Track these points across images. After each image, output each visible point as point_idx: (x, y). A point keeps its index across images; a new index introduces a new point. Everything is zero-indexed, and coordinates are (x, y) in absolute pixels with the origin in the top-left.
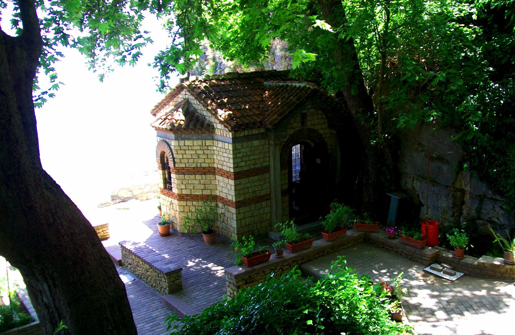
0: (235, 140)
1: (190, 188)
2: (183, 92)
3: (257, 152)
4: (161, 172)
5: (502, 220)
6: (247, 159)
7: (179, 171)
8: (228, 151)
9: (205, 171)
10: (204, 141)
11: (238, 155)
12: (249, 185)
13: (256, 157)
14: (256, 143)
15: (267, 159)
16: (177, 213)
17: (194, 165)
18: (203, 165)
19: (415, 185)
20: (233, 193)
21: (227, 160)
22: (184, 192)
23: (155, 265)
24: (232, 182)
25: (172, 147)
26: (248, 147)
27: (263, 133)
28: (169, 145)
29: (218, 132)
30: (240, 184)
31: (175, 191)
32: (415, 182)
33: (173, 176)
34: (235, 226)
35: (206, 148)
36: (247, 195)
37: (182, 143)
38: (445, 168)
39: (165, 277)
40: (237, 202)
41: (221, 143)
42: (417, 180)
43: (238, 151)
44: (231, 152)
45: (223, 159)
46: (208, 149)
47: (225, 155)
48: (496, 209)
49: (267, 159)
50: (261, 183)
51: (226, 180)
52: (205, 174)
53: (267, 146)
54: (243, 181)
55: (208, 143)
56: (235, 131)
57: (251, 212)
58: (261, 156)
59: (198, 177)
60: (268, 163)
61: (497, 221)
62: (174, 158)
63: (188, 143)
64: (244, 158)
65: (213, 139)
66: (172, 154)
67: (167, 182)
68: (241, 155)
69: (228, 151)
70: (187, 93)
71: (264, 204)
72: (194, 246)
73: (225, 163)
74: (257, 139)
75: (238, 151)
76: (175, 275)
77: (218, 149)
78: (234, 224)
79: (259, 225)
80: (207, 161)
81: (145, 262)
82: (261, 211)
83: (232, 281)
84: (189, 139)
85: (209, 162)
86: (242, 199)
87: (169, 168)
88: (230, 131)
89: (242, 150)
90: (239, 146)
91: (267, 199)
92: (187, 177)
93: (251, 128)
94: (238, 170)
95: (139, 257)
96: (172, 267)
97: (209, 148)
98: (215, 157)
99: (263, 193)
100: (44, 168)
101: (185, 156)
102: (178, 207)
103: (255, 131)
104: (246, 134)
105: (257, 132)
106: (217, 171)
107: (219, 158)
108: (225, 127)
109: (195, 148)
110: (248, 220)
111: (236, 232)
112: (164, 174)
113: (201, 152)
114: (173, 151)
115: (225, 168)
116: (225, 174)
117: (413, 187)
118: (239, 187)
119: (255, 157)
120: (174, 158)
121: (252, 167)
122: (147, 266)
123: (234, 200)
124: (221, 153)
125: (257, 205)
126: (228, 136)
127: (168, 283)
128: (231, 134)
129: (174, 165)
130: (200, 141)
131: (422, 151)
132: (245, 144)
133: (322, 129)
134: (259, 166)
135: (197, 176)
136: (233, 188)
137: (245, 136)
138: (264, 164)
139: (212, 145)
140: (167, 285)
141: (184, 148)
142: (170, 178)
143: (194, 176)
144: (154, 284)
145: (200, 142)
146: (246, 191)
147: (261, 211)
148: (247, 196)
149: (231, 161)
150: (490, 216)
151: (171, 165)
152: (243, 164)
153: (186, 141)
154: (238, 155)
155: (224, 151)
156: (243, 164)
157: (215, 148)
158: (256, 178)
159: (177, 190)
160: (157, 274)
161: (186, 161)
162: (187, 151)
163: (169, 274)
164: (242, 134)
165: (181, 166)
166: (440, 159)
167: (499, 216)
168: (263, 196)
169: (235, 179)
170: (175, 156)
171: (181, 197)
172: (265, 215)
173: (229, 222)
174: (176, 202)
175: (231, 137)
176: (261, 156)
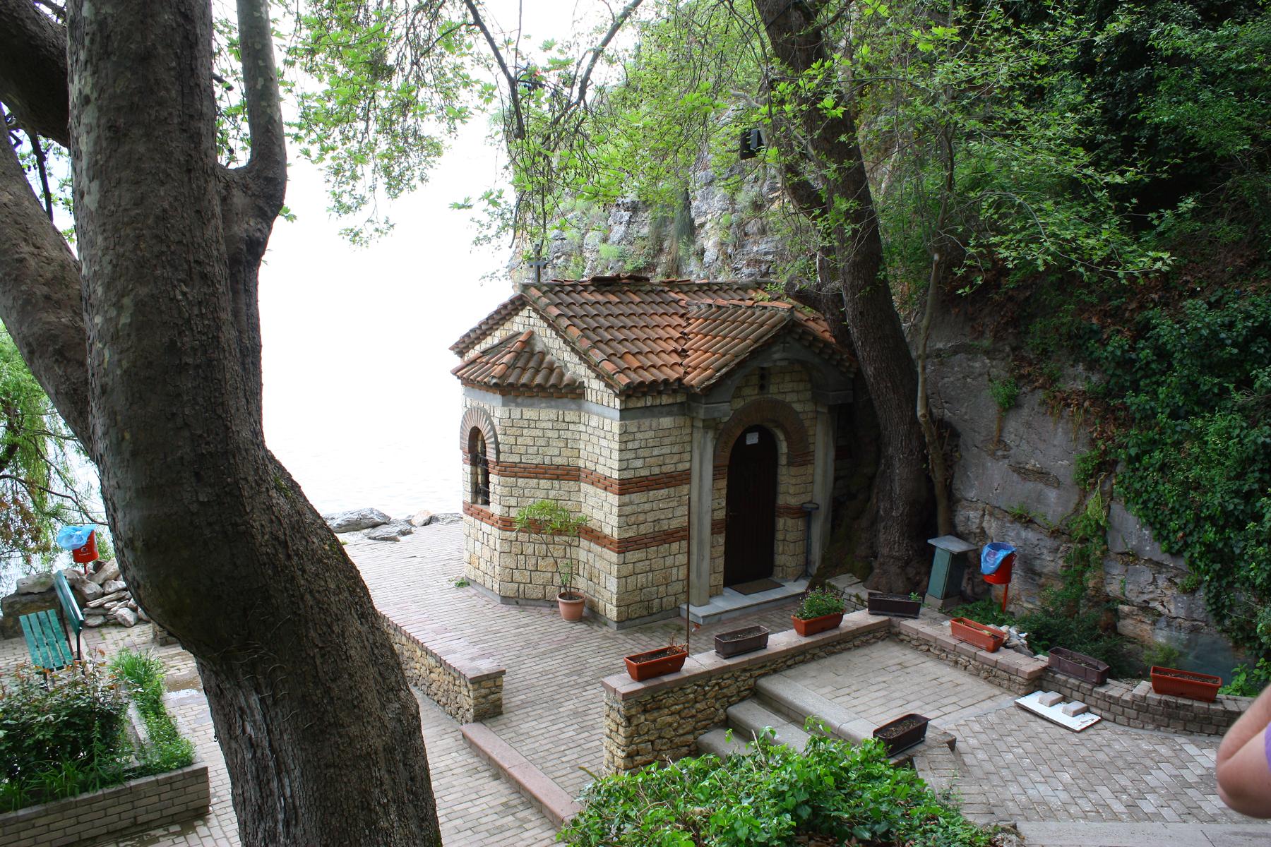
0: (625, 413)
2: (525, 313)
3: (667, 441)
4: (468, 468)
5: (1172, 607)
6: (646, 453)
8: (609, 436)
9: (559, 472)
11: (630, 445)
12: (647, 507)
13: (666, 450)
14: (666, 422)
15: (687, 456)
16: (497, 554)
17: (538, 460)
18: (558, 461)
19: (985, 525)
20: (614, 520)
21: (606, 452)
23: (449, 659)
24: (614, 499)
25: (496, 421)
26: (651, 429)
27: (682, 403)
28: (489, 417)
29: (591, 396)
30: (631, 503)
31: (495, 508)
32: (987, 517)
33: (493, 478)
34: (614, 589)
35: (564, 426)
36: (642, 527)
37: (516, 413)
38: (1052, 495)
39: (470, 686)
40: (621, 541)
41: (595, 418)
42: (991, 514)
43: (631, 437)
44: (617, 438)
45: (598, 451)
47: (604, 443)
48: (1160, 583)
49: (687, 456)
50: (672, 504)
51: (601, 492)
52: (558, 478)
53: (689, 431)
54: (636, 497)
56: (628, 397)
57: (647, 562)
58: (676, 449)
59: (544, 483)
60: (687, 465)
61: (1160, 608)
62: (497, 443)
63: (529, 413)
64: (641, 453)
65: (580, 409)
66: (495, 436)
67: (481, 491)
68: (636, 445)
69: (609, 436)
70: (533, 314)
71: (675, 546)
72: (528, 625)
73: (602, 460)
74: (669, 414)
75: (631, 437)
76: (490, 683)
77: (590, 431)
78: (612, 585)
79: (662, 589)
80: (565, 452)
81: (427, 652)
82: (669, 561)
83: (615, 705)
84: (531, 405)
86: (631, 534)
87: (486, 462)
88: (616, 395)
89: (638, 435)
90: (632, 426)
91: (682, 538)
93: (660, 393)
94: (627, 475)
95: (416, 642)
96: (486, 666)
97: (572, 427)
98: (582, 446)
99: (675, 524)
100: (269, 445)
101: (520, 440)
102: (498, 541)
103: (665, 400)
104: (649, 404)
105: (671, 401)
106: (583, 475)
107: (590, 448)
108: (608, 386)
109: (544, 425)
110: (641, 579)
111: (614, 602)
112: (474, 474)
113: (553, 434)
114: (498, 428)
115: (601, 470)
116: (601, 482)
117: (982, 529)
118: (628, 510)
119: (664, 451)
120: (497, 443)
121: (656, 470)
122: (432, 662)
123: (616, 536)
124: (594, 439)
125: (662, 548)
126: (612, 405)
127: (475, 698)
128: (617, 401)
129: (498, 458)
131: (1004, 457)
132: (646, 423)
133: (799, 401)
134: (668, 469)
136: (615, 510)
137: (646, 407)
138: (681, 467)
140: (471, 702)
141: (521, 423)
142: (487, 483)
144: (444, 700)
145: (552, 414)
146: (642, 517)
147: (669, 561)
148: (643, 529)
149: (616, 455)
150: (1146, 597)
151: (491, 455)
152: (639, 463)
154: (630, 445)
155: (602, 434)
156: (639, 463)
157: (582, 428)
158: (664, 492)
159: (499, 507)
160: (451, 679)
161: (523, 451)
162: (525, 431)
163: (477, 681)
164: (641, 404)
166: (1042, 475)
167: (1165, 599)
168: (677, 531)
169: (621, 493)
170: (500, 438)
171: (506, 524)
172: (675, 570)
173: (602, 576)
174: (496, 532)
175: (618, 407)
176: (676, 449)
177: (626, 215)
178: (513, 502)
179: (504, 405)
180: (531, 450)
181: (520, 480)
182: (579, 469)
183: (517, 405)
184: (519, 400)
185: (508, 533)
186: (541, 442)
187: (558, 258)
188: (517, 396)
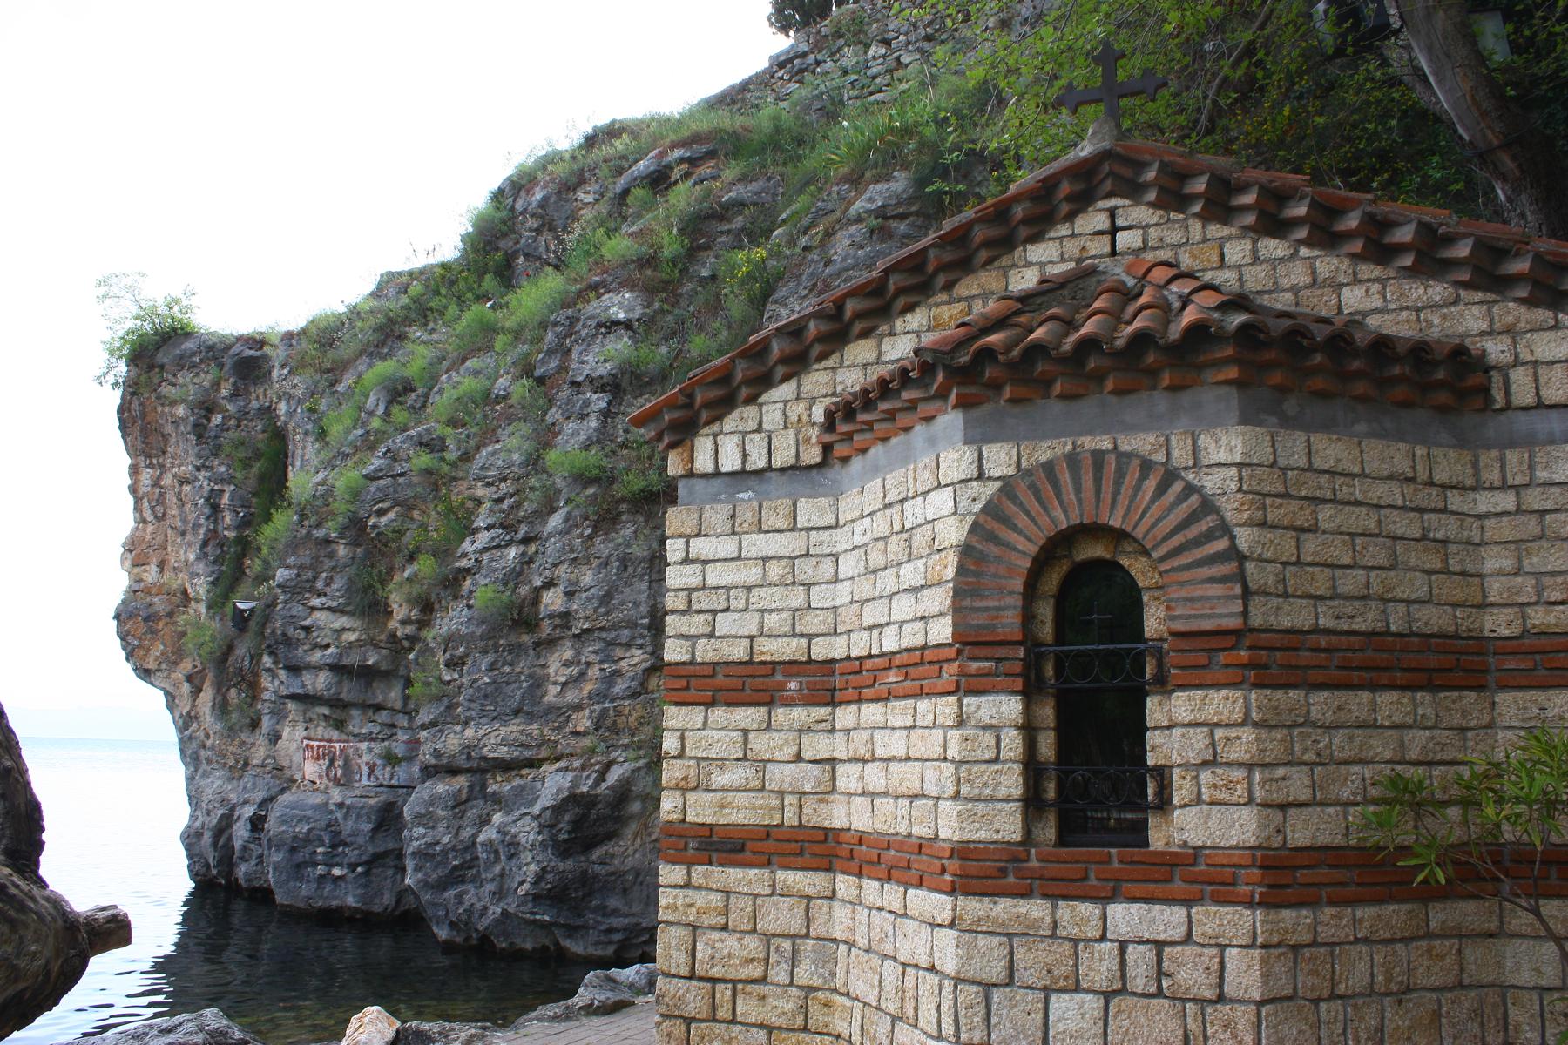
1: (1346, 794)
7: (1267, 660)
9: (1433, 660)
10: (1420, 451)
22: (1304, 831)
37: (1293, 446)
46: (1444, 511)
55: (1449, 464)
59: (1390, 705)
63: (1331, 450)
84: (1327, 426)
85: (1459, 595)
92: (1321, 703)
97: (1455, 501)
101: (1311, 545)
109: (1379, 492)
113: (1404, 525)
130: (1403, 446)
135: (1386, 699)
139: (1469, 482)
143: (1365, 696)
153: (1320, 441)
165: (1285, 622)
170: (1245, 538)
171: (1281, 876)
177: (599, 401)
178: (1298, 785)
179: (1244, 420)
180: (1350, 582)
181: (1319, 697)
182: (1480, 643)
183: (1288, 423)
184: (1291, 406)
185: (1286, 913)
186: (1375, 553)
187: (381, 513)
188: (1283, 390)
